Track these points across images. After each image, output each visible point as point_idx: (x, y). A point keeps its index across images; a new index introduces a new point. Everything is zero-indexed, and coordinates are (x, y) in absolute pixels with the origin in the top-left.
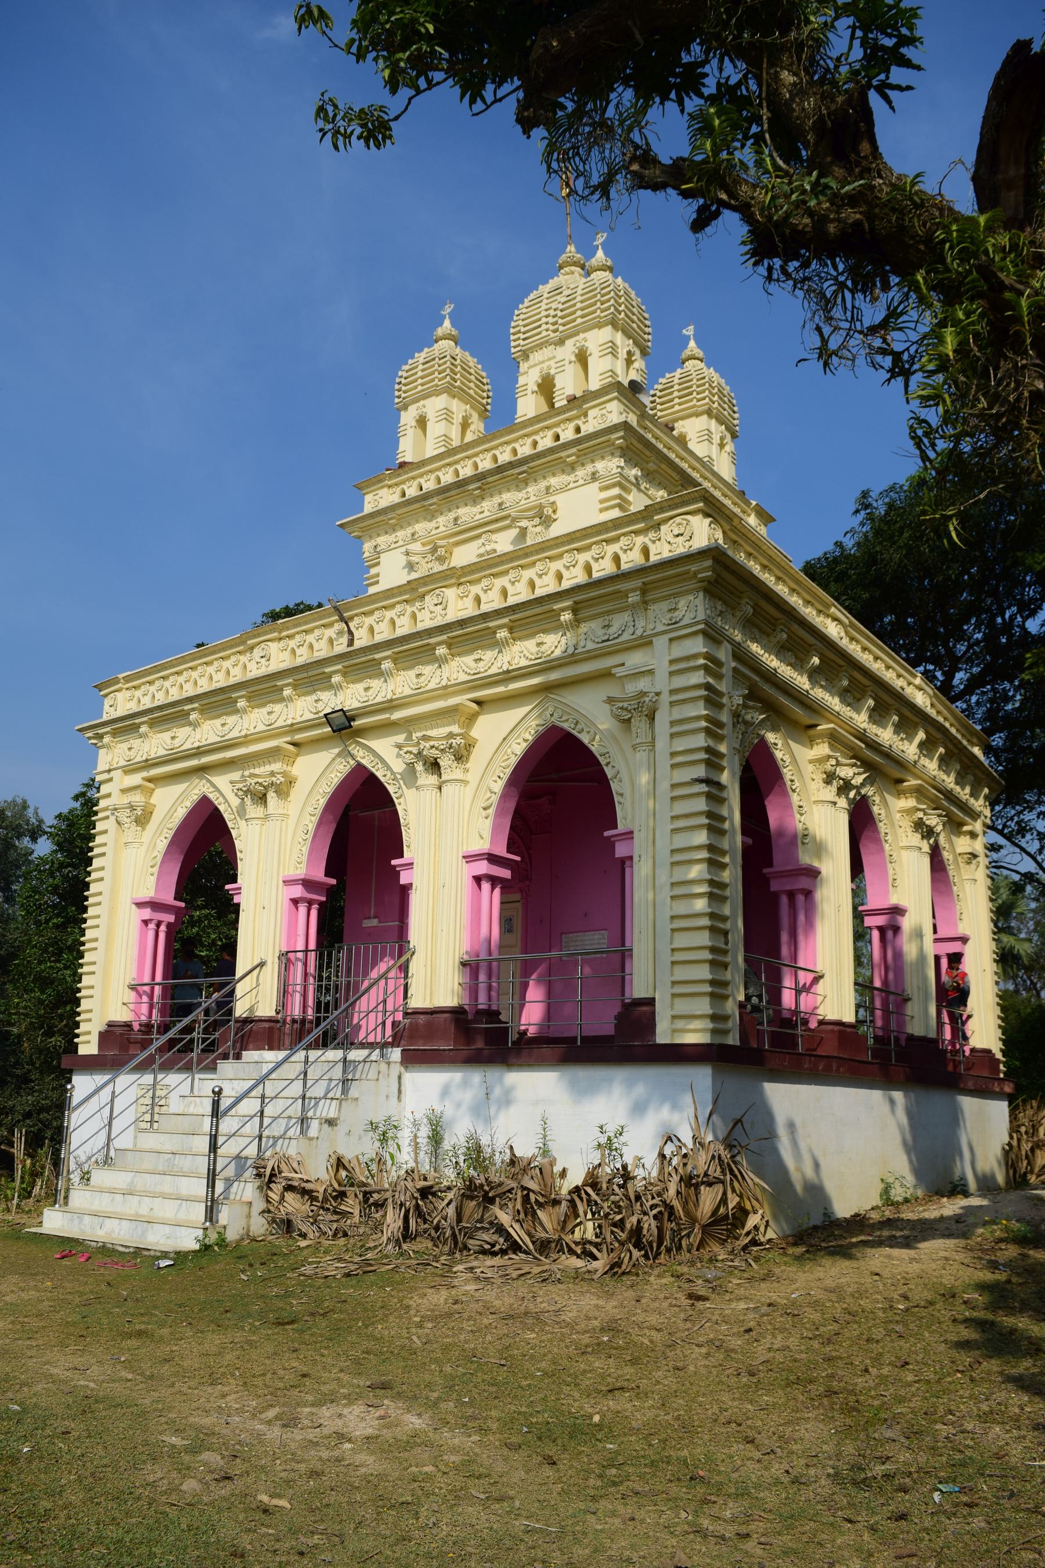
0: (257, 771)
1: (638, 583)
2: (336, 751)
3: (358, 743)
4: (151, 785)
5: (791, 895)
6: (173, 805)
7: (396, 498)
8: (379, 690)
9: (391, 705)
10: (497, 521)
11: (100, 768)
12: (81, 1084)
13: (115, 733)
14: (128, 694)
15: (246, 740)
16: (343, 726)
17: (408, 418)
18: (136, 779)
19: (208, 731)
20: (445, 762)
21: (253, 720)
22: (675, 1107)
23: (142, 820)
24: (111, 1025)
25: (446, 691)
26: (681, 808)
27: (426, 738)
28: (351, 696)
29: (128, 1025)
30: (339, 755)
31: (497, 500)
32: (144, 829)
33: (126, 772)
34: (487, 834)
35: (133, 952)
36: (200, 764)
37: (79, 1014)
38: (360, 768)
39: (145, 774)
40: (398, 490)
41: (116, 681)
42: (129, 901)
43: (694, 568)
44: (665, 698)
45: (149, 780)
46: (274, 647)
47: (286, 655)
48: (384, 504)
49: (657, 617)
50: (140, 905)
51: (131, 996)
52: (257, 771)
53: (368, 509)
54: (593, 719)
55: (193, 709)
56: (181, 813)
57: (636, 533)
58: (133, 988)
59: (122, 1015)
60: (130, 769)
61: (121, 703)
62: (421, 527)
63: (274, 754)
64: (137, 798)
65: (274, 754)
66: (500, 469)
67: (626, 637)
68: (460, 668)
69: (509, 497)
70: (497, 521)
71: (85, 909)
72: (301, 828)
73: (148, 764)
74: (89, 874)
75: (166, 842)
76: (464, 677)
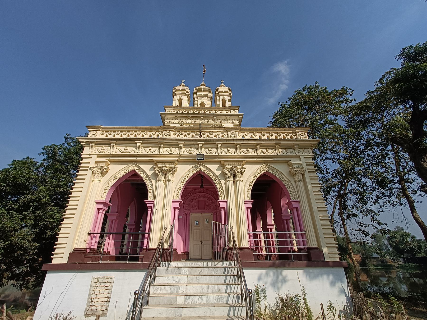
0: (168, 166)
1: (299, 143)
2: (193, 166)
3: (201, 164)
4: (109, 163)
5: (287, 220)
6: (118, 171)
7: (175, 112)
8: (213, 152)
9: (219, 156)
10: (205, 125)
11: (84, 153)
12: (50, 278)
13: (95, 143)
14: (102, 133)
15: (160, 156)
16: (199, 160)
17: (177, 98)
18: (104, 159)
19: (143, 151)
20: (238, 175)
21: (164, 151)
22: (342, 282)
23: (103, 174)
24: (75, 250)
25: (238, 156)
26: (317, 197)
27: (236, 167)
28: (204, 151)
29: (85, 250)
30: (194, 167)
31: (206, 121)
32: (103, 177)
33: (98, 157)
34: (250, 196)
35: (92, 220)
36: (136, 160)
37: (56, 245)
38: (200, 171)
39: (108, 159)
40: (176, 111)
41: (99, 127)
42: (93, 201)
43: (313, 143)
44: (307, 171)
45: (110, 161)
46: (172, 133)
47: (176, 136)
48: (171, 112)
49: (299, 152)
50: (97, 203)
51: (88, 238)
52: (168, 166)
53: (166, 112)
54: (281, 172)
55: (139, 143)
56: (123, 174)
57: (290, 133)
58: (89, 234)
59: (82, 245)
60: (99, 156)
61: (99, 134)
62: (184, 121)
63: (172, 162)
64: (104, 165)
65: (172, 162)
66: (210, 114)
67: (292, 154)
68: (242, 152)
69: (210, 121)
70: (205, 125)
71: (68, 202)
72: (178, 186)
73: (111, 155)
74: (72, 189)
75: (113, 183)
76: (243, 154)
